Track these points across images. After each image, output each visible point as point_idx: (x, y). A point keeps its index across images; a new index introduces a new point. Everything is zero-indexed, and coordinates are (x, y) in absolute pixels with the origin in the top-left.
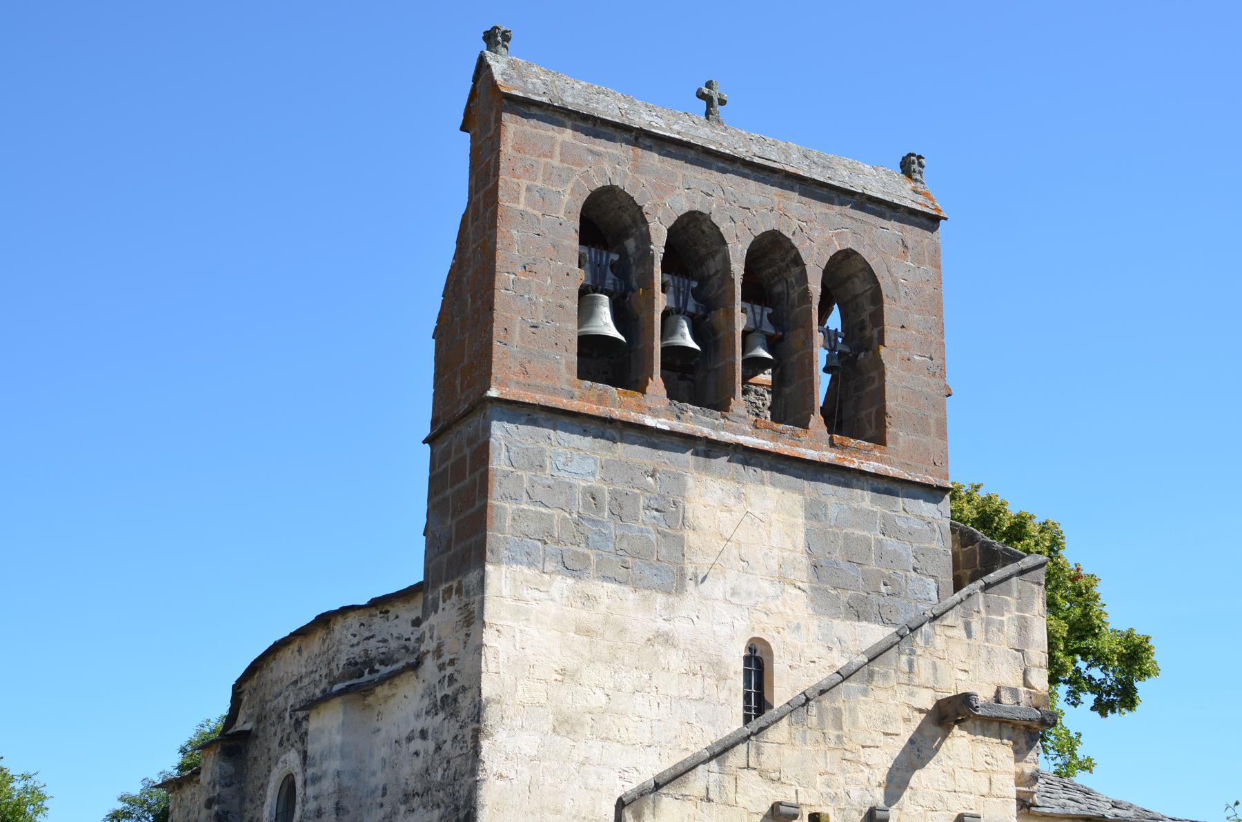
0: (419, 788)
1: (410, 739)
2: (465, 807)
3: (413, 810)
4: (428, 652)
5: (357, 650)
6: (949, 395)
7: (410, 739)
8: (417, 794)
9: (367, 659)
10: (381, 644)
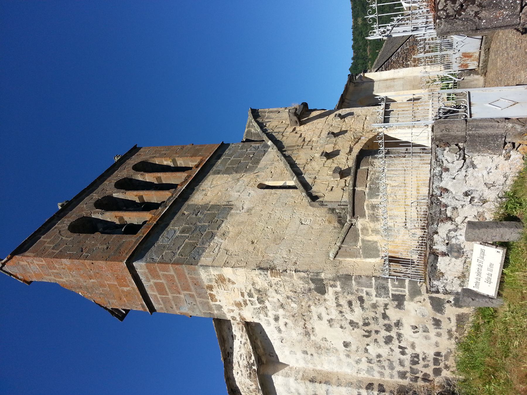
0: (302, 323)
1: (280, 331)
2: (308, 283)
3: (313, 328)
4: (239, 314)
5: (244, 371)
6: (193, 144)
7: (280, 331)
8: (305, 324)
9: (248, 366)
10: (242, 358)
